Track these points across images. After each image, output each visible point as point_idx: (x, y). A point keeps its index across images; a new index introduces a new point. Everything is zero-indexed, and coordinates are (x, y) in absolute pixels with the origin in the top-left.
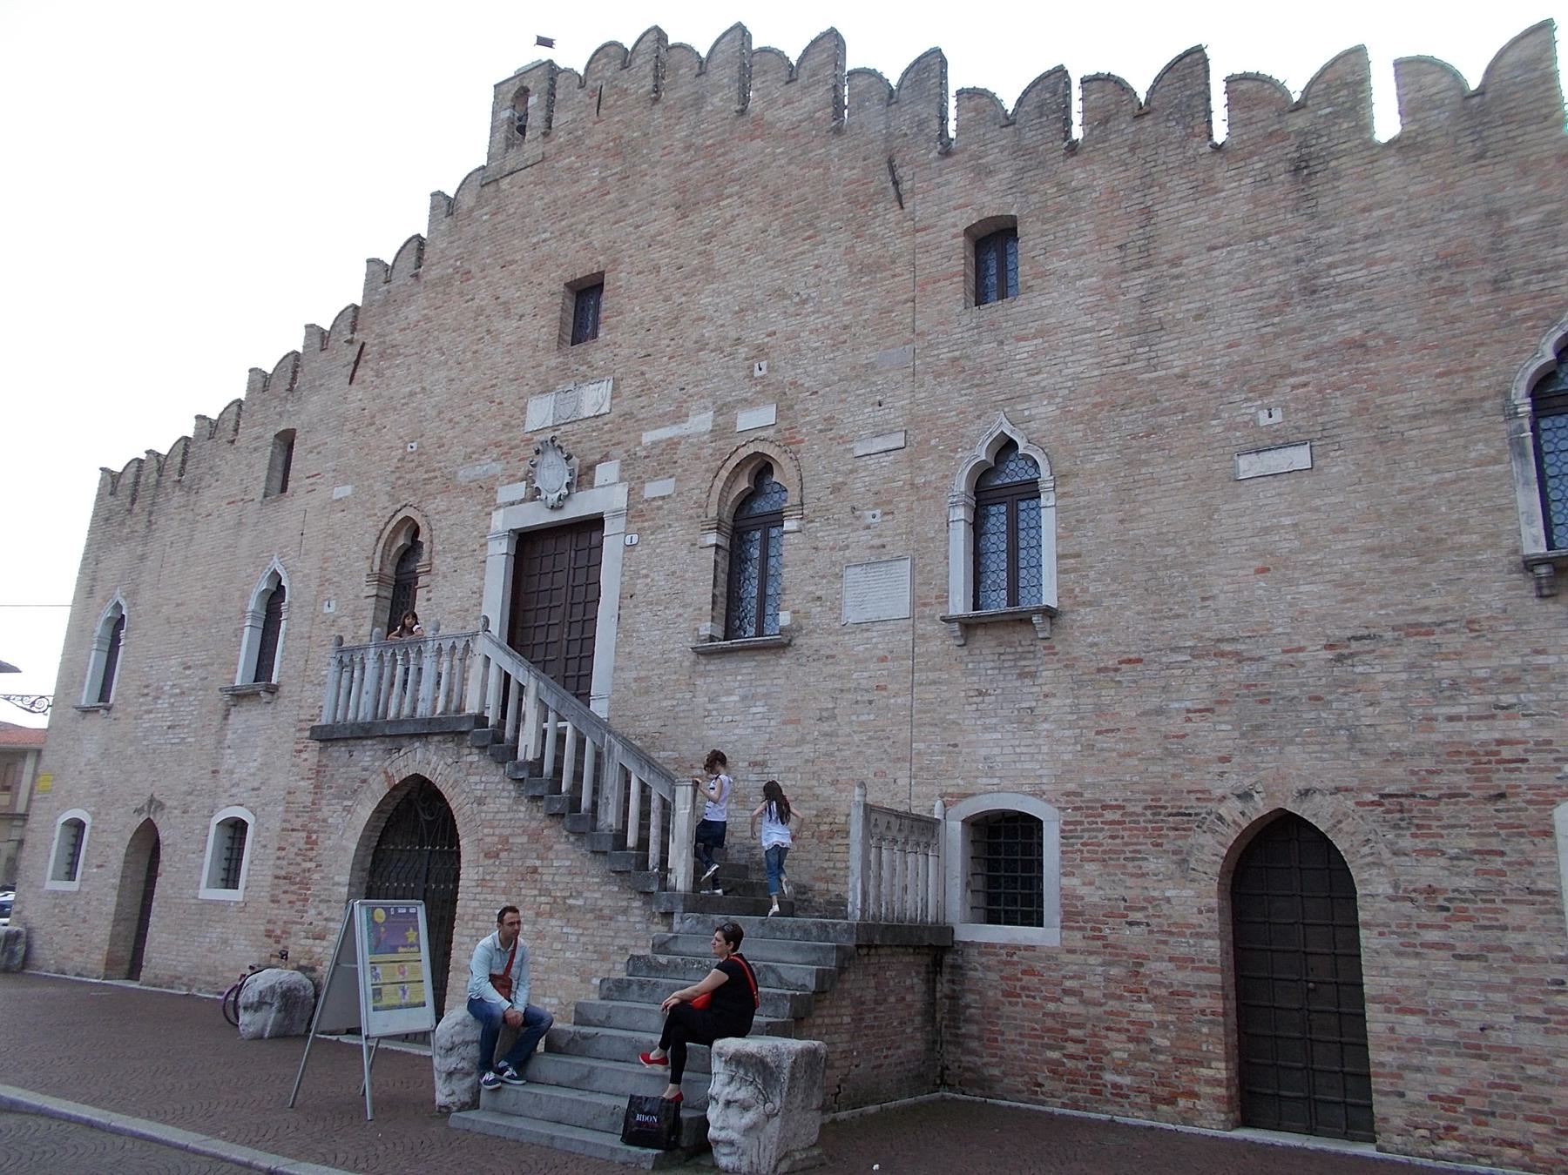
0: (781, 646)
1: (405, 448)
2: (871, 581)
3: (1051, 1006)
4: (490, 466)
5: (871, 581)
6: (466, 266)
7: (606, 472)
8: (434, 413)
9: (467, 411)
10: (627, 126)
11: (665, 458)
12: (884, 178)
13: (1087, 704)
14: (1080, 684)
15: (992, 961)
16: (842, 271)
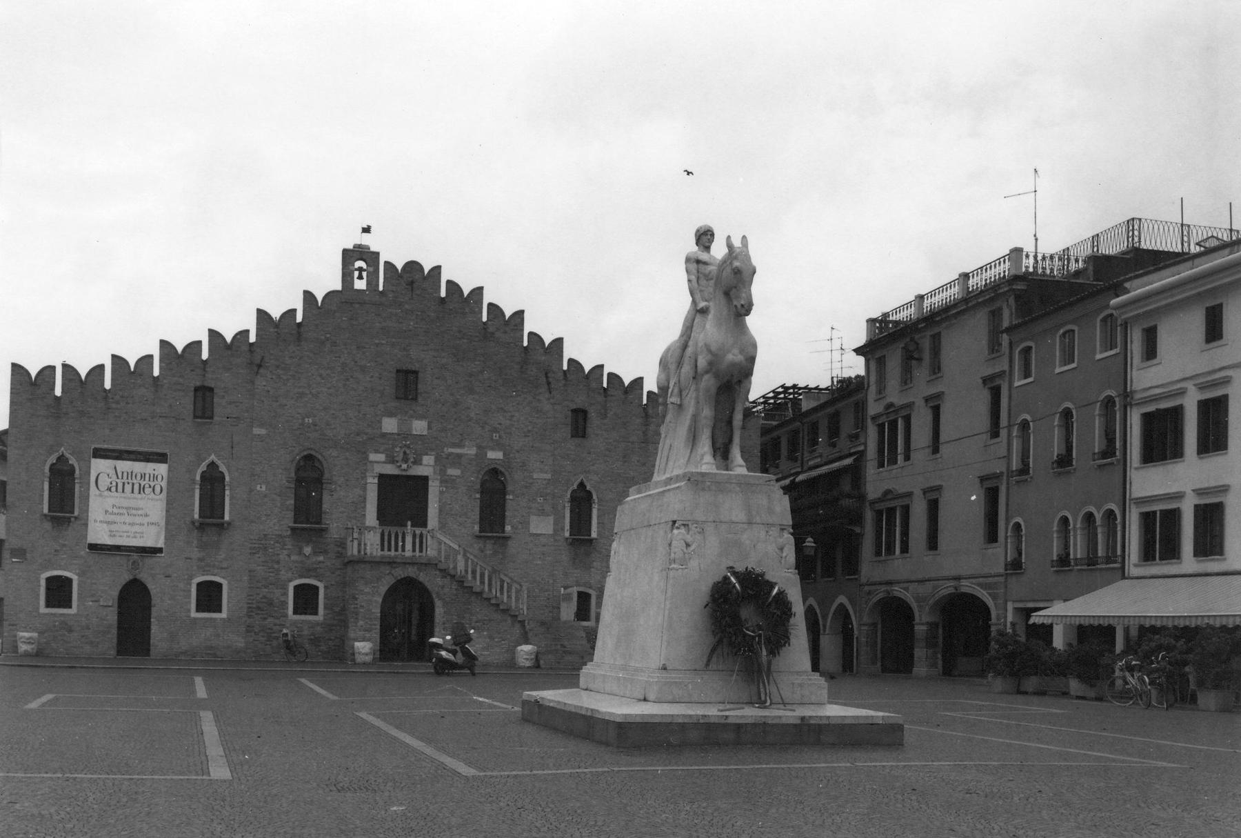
7: (428, 460)
11: (457, 460)
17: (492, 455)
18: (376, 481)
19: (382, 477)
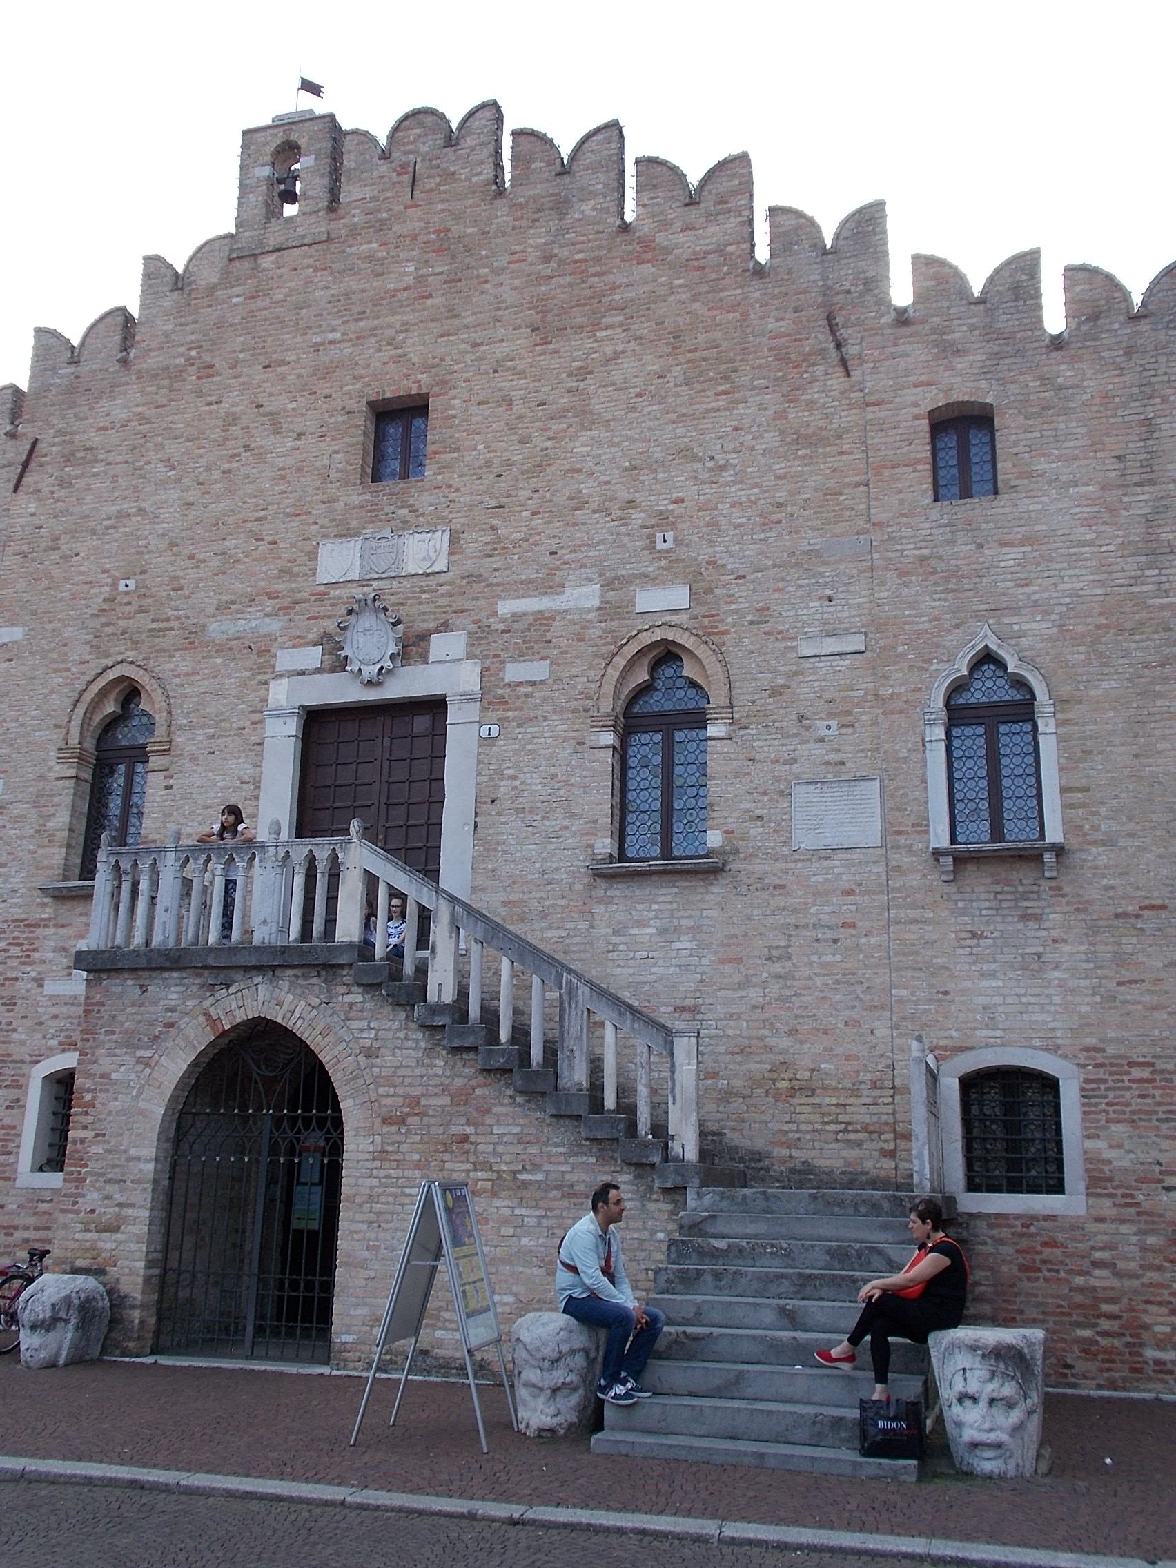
0: (710, 869)
1: (114, 585)
2: (827, 800)
3: (1079, 1281)
4: (258, 622)
5: (827, 800)
6: (207, 358)
8: (163, 544)
9: (219, 547)
10: (457, 218)
11: (535, 635)
12: (822, 338)
13: (1105, 952)
14: (1096, 930)
15: (1005, 1233)
16: (771, 438)
17: (649, 600)
18: (292, 727)
19: (316, 720)
